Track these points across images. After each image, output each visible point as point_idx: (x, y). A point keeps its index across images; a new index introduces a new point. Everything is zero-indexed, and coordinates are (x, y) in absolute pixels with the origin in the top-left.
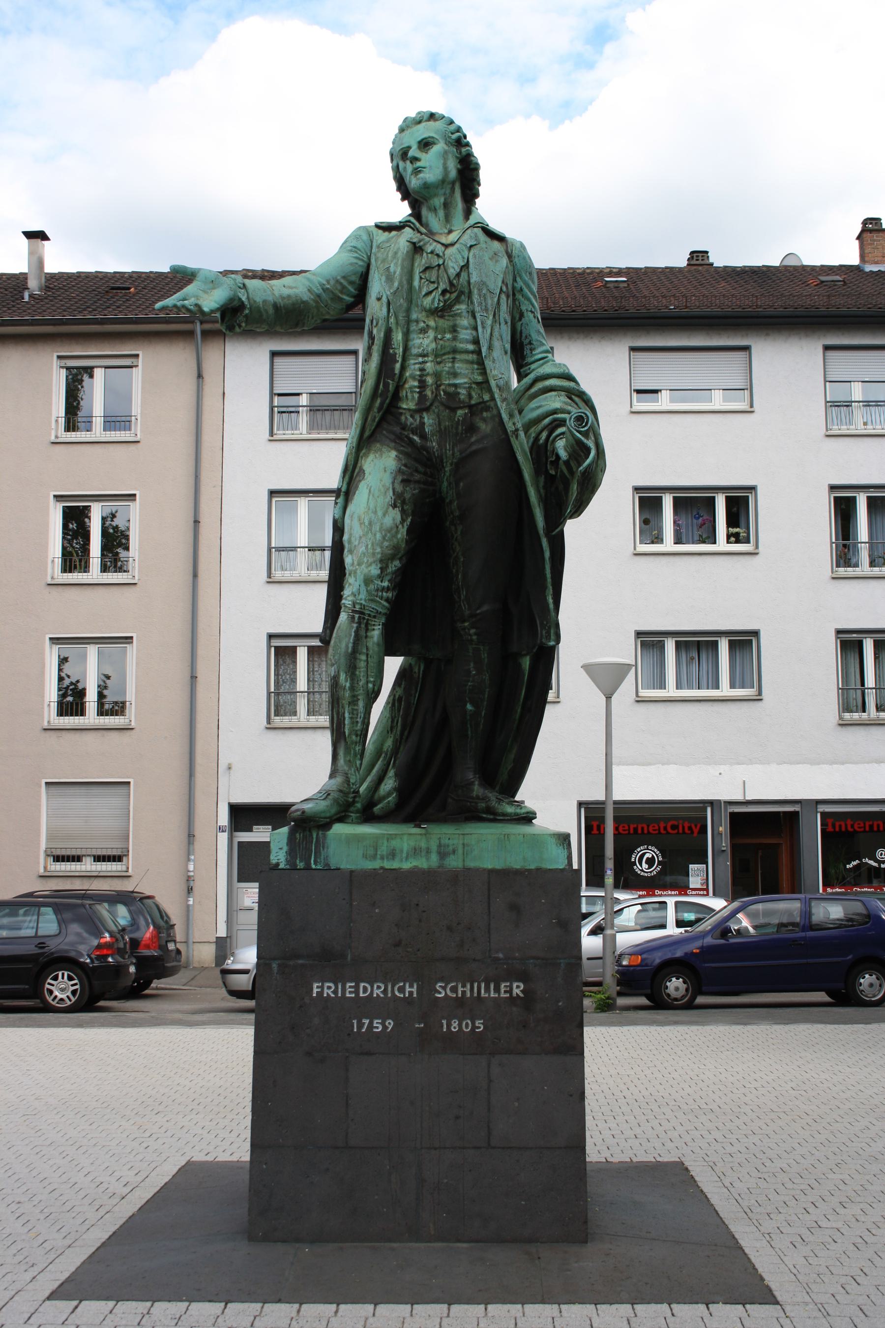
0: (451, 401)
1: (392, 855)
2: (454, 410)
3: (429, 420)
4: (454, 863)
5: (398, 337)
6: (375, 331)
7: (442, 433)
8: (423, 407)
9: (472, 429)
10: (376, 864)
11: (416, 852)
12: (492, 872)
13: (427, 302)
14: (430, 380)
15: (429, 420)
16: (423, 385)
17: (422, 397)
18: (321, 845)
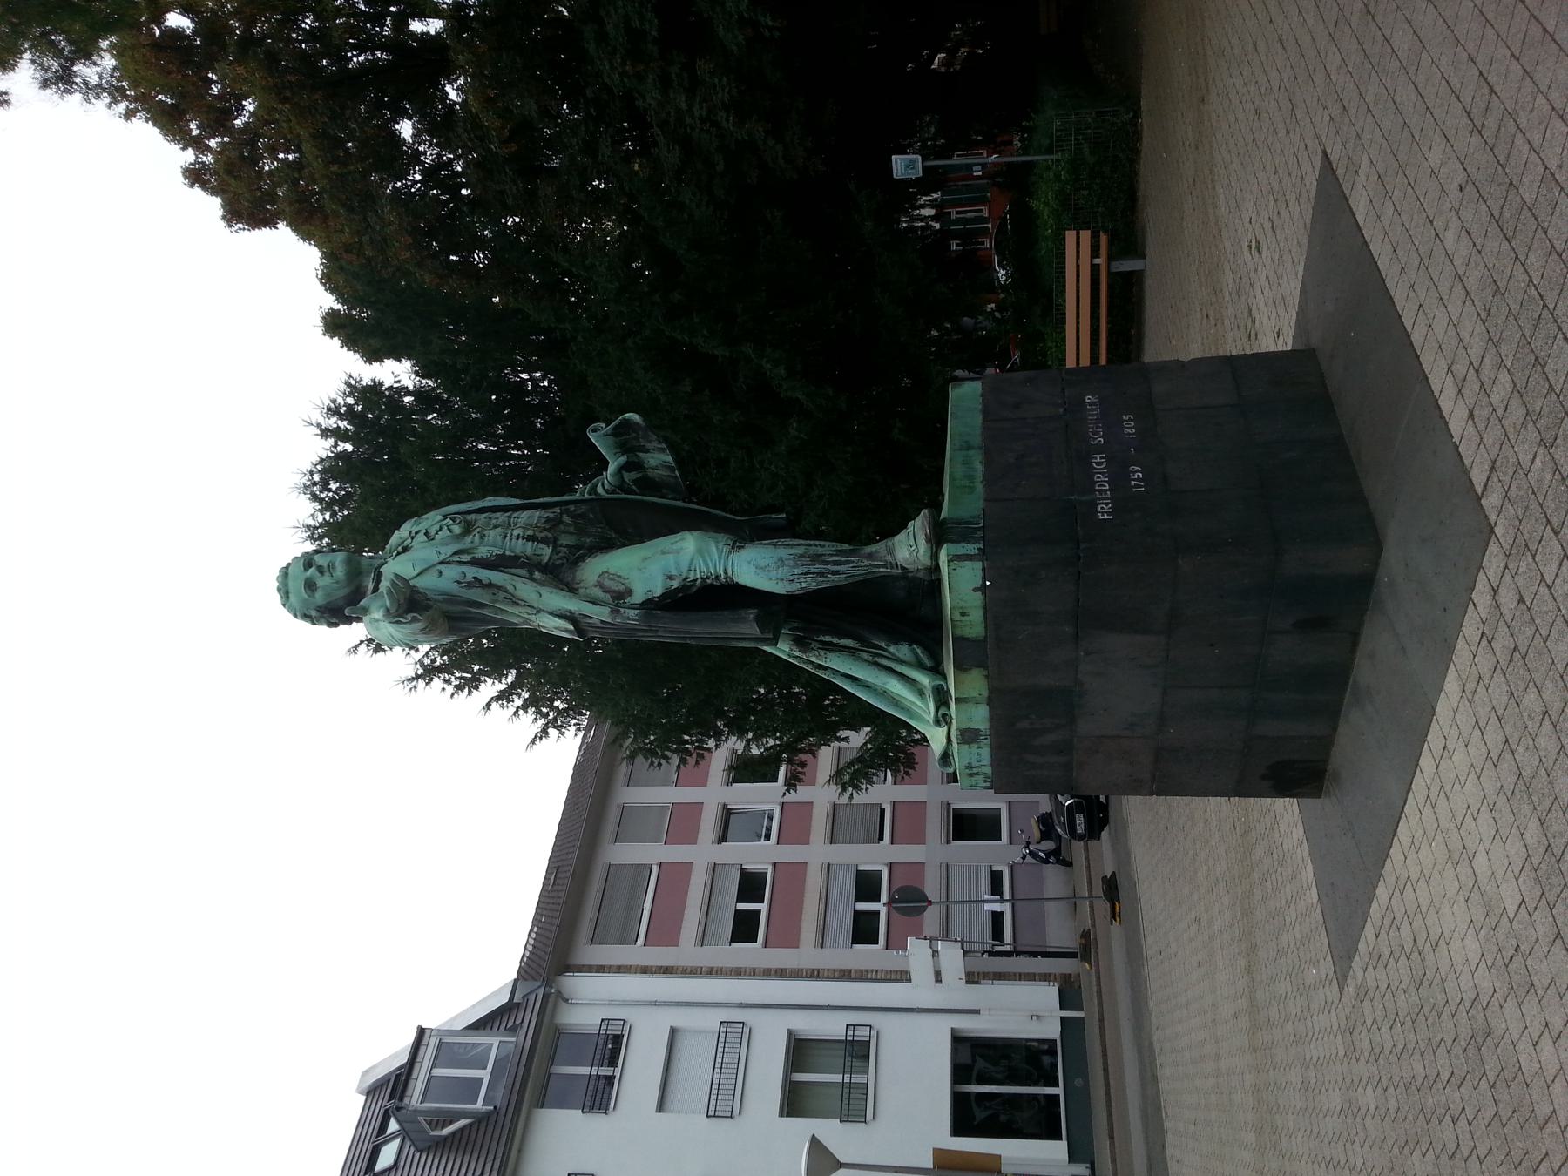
0: (554, 523)
1: (971, 478)
2: (561, 522)
3: (565, 540)
4: (978, 439)
5: (483, 552)
6: (469, 577)
7: (581, 532)
8: (554, 542)
9: (582, 516)
10: (979, 488)
11: (967, 463)
12: (985, 419)
13: (457, 529)
14: (530, 533)
15: (565, 540)
16: (532, 538)
17: (545, 541)
18: (959, 522)
